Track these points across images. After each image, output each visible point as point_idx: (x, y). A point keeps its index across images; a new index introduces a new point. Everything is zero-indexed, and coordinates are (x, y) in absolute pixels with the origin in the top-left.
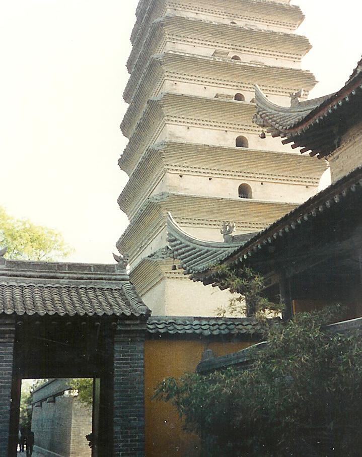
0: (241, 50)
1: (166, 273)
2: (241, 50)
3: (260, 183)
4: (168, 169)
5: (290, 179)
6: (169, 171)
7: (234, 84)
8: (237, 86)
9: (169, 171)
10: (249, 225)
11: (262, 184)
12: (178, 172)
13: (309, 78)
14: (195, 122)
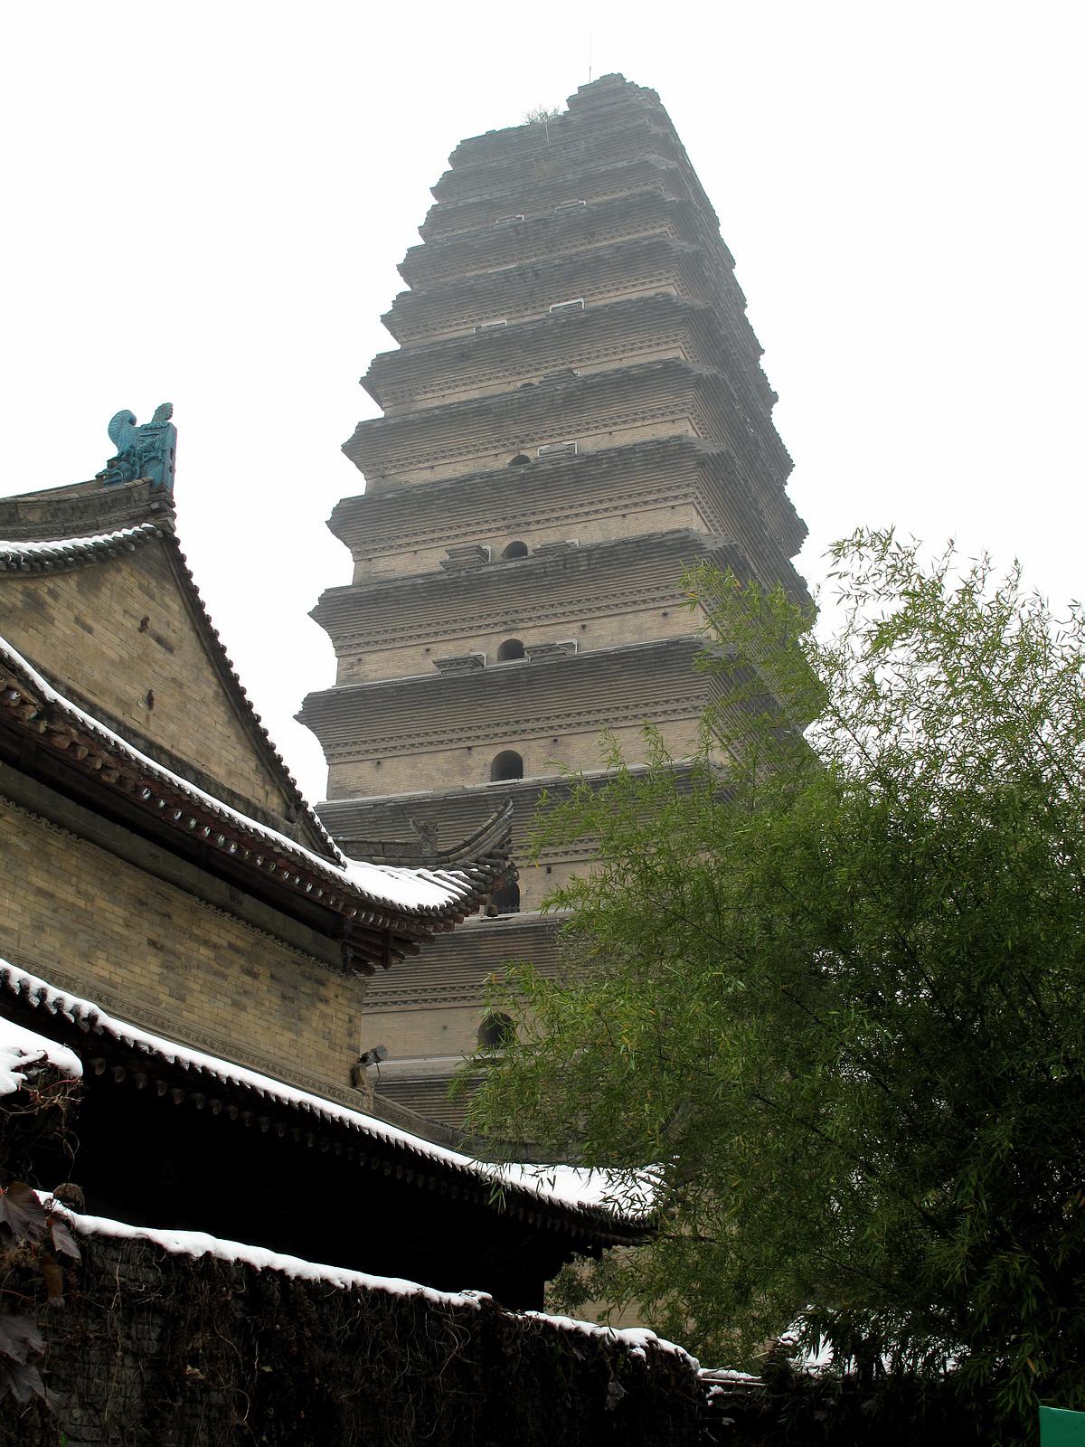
0: (528, 524)
2: (528, 524)
3: (545, 868)
7: (498, 619)
8: (505, 623)
11: (549, 871)
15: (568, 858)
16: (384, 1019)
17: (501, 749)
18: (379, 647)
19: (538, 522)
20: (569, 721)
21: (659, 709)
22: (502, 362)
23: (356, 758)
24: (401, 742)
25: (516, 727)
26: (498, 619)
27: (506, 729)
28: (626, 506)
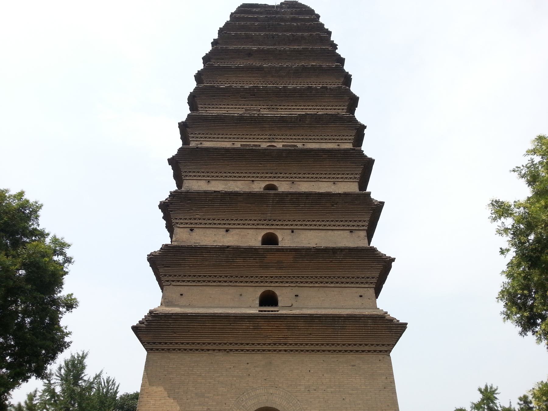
0: (277, 109)
1: (148, 343)
2: (277, 109)
3: (291, 231)
4: (177, 223)
5: (328, 223)
6: (178, 225)
7: (267, 137)
9: (178, 225)
10: (272, 280)
11: (293, 232)
12: (187, 226)
13: (351, 121)
14: (217, 174)
15: (302, 227)
16: (207, 289)
17: (267, 183)
18: (211, 140)
19: (282, 109)
20: (300, 176)
21: (340, 176)
22: (264, 60)
23: (198, 178)
24: (221, 174)
25: (275, 175)
26: (267, 137)
27: (270, 175)
28: (318, 109)
